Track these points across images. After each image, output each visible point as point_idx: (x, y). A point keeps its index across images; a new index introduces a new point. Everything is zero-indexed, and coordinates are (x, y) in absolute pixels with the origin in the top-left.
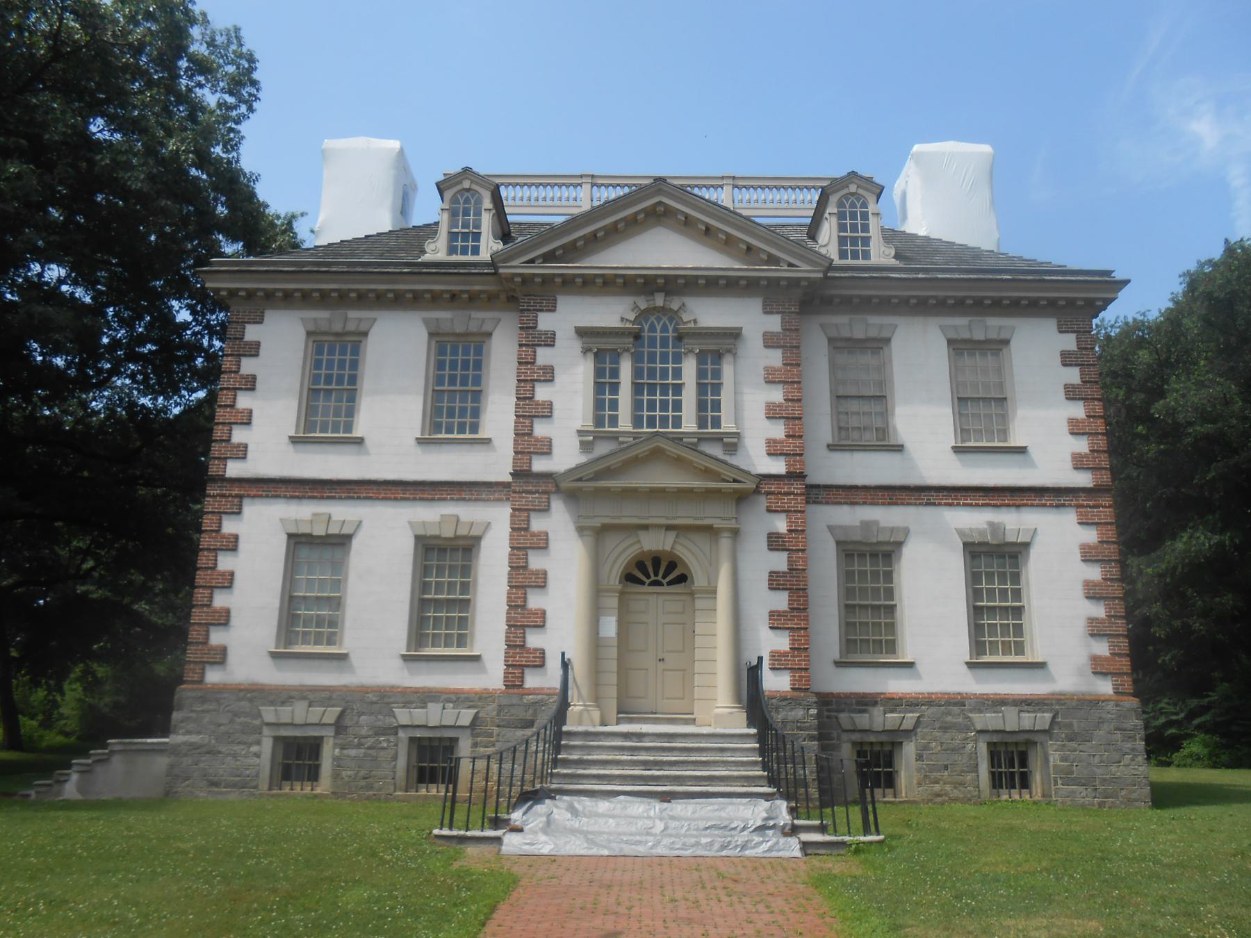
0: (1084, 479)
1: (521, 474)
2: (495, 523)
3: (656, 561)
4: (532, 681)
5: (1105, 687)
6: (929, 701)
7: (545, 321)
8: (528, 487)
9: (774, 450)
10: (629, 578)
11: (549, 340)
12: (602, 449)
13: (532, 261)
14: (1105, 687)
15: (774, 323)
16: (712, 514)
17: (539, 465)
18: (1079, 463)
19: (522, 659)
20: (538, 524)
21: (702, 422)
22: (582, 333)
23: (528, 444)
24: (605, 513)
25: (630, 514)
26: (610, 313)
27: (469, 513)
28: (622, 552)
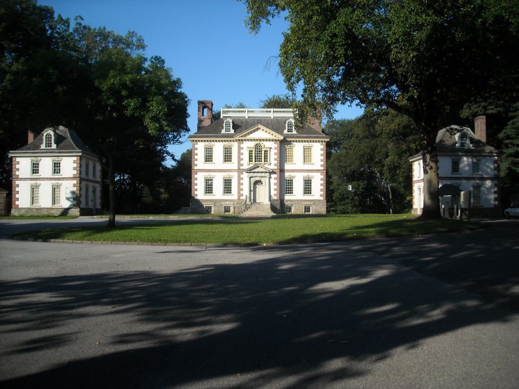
0: (322, 168)
1: (239, 169)
4: (242, 198)
5: (322, 198)
6: (297, 200)
7: (242, 146)
14: (322, 198)
17: (242, 168)
18: (322, 166)
19: (240, 195)
20: (242, 176)
21: (265, 161)
23: (240, 165)
24: (251, 175)
25: (255, 175)
26: (252, 144)
27: (231, 174)
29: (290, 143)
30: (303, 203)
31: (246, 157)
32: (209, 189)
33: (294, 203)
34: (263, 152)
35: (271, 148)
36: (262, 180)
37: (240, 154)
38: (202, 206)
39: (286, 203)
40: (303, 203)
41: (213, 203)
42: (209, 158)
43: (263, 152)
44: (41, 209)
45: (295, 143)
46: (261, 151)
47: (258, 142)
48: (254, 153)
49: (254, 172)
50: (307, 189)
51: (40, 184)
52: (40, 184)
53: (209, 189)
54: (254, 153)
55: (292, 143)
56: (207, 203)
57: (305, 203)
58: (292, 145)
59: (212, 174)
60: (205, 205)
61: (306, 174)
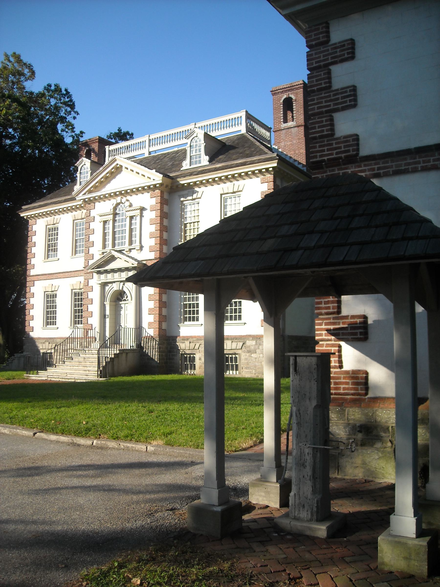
13: (85, 194)
24: (103, 278)
25: (110, 277)
29: (189, 189)
32: (50, 319)
33: (197, 347)
35: (142, 209)
38: (38, 351)
39: (183, 346)
42: (51, 248)
45: (203, 188)
47: (119, 199)
49: (106, 272)
55: (197, 189)
58: (195, 196)
60: (43, 348)
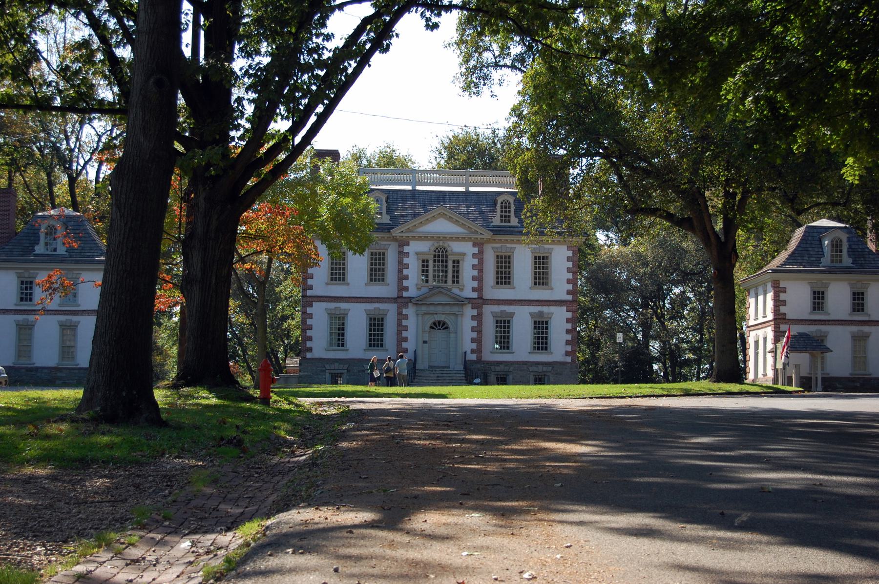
2: (391, 309)
3: (439, 322)
6: (517, 363)
7: (406, 249)
8: (401, 301)
9: (474, 290)
10: (431, 327)
11: (407, 255)
12: (424, 290)
15: (476, 250)
16: (455, 309)
17: (405, 294)
20: (405, 312)
21: (453, 282)
22: (417, 254)
24: (424, 309)
25: (432, 309)
26: (424, 247)
28: (430, 320)
30: (531, 369)
31: (413, 272)
33: (511, 368)
34: (450, 264)
36: (449, 320)
37: (402, 266)
40: (531, 369)
41: (346, 366)
43: (450, 264)
44: (37, 369)
46: (446, 262)
48: (431, 263)
50: (541, 342)
51: (79, 322)
52: (79, 322)
53: (339, 337)
54: (431, 263)
56: (332, 367)
57: (534, 369)
59: (344, 306)
61: (535, 309)
